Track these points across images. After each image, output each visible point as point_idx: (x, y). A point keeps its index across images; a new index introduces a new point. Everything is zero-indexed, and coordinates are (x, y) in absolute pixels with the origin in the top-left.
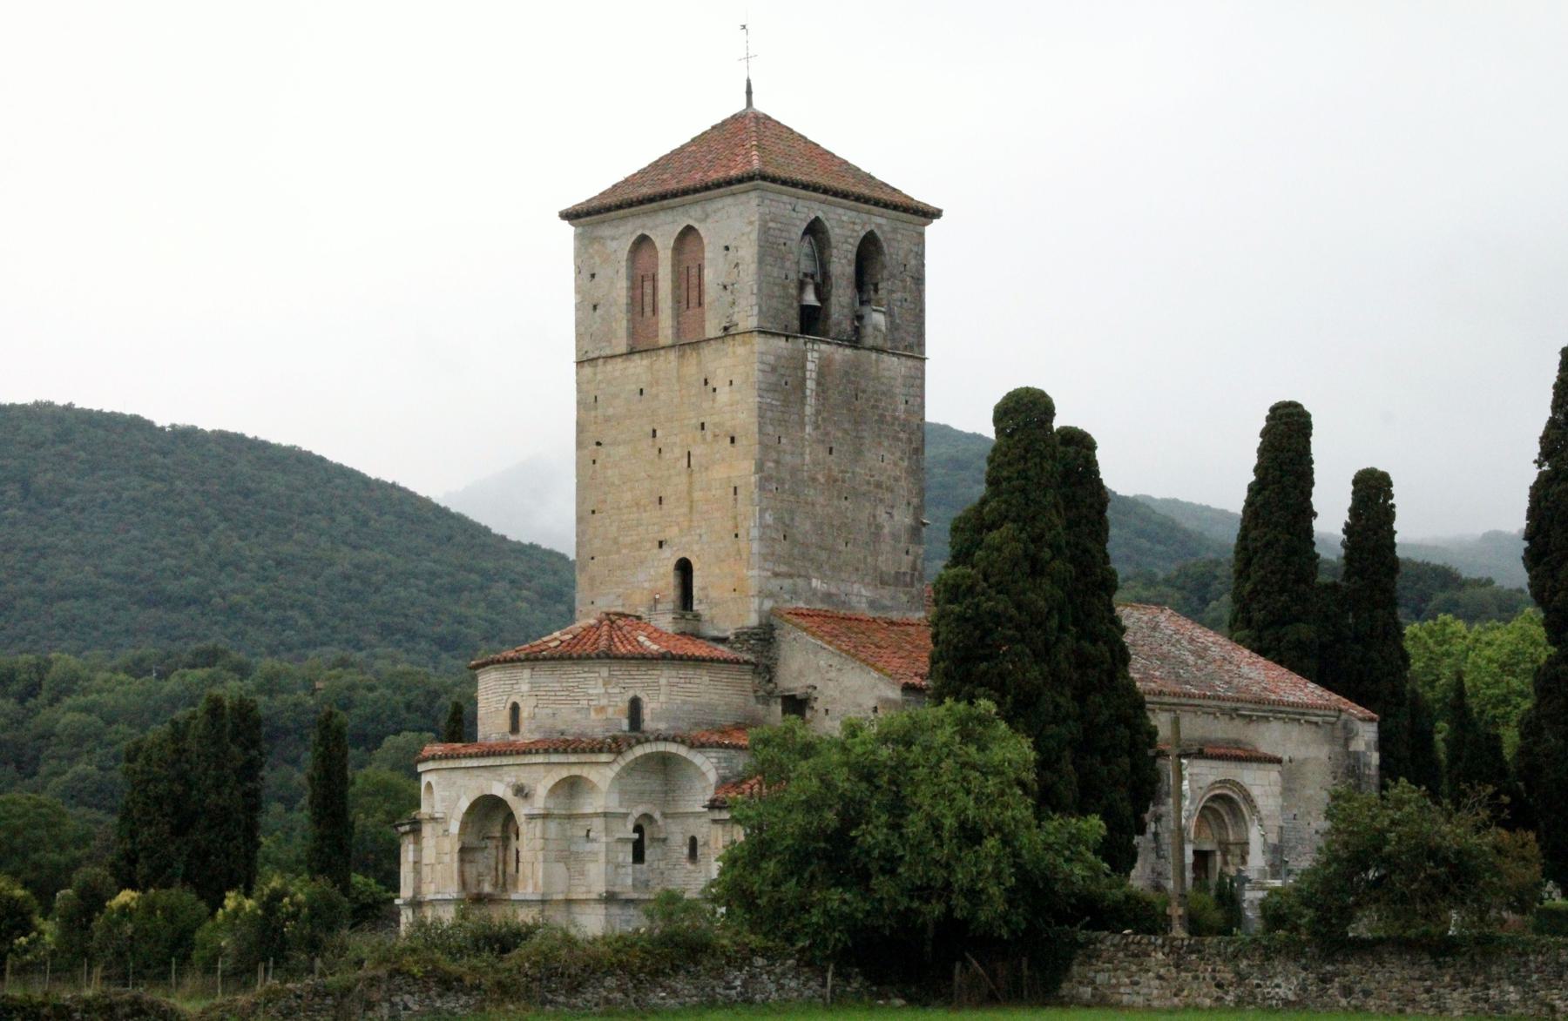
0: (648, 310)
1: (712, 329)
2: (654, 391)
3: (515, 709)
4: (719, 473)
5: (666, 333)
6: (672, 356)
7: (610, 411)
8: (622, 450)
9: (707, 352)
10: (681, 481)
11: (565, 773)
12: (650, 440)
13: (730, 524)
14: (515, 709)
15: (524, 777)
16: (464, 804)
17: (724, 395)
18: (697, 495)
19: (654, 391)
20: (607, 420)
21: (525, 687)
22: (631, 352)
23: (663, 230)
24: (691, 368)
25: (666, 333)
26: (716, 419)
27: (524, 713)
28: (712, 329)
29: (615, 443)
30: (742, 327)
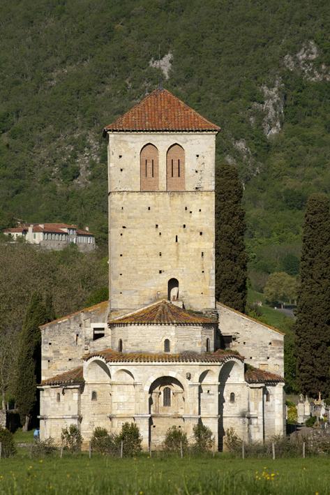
0: (150, 175)
1: (189, 186)
2: (156, 209)
3: (167, 342)
4: (193, 246)
5: (162, 184)
6: (167, 195)
7: (131, 215)
8: (138, 231)
9: (187, 197)
10: (173, 247)
11: (205, 369)
12: (155, 229)
13: (200, 266)
14: (167, 342)
15: (188, 370)
16: (153, 379)
17: (196, 215)
18: (181, 254)
19: (156, 209)
20: (129, 218)
21: (173, 334)
22: (142, 192)
23: (163, 142)
24: (178, 201)
25: (162, 184)
26: (192, 224)
27: (172, 344)
28: (189, 186)
29: (134, 228)
30: (206, 188)
